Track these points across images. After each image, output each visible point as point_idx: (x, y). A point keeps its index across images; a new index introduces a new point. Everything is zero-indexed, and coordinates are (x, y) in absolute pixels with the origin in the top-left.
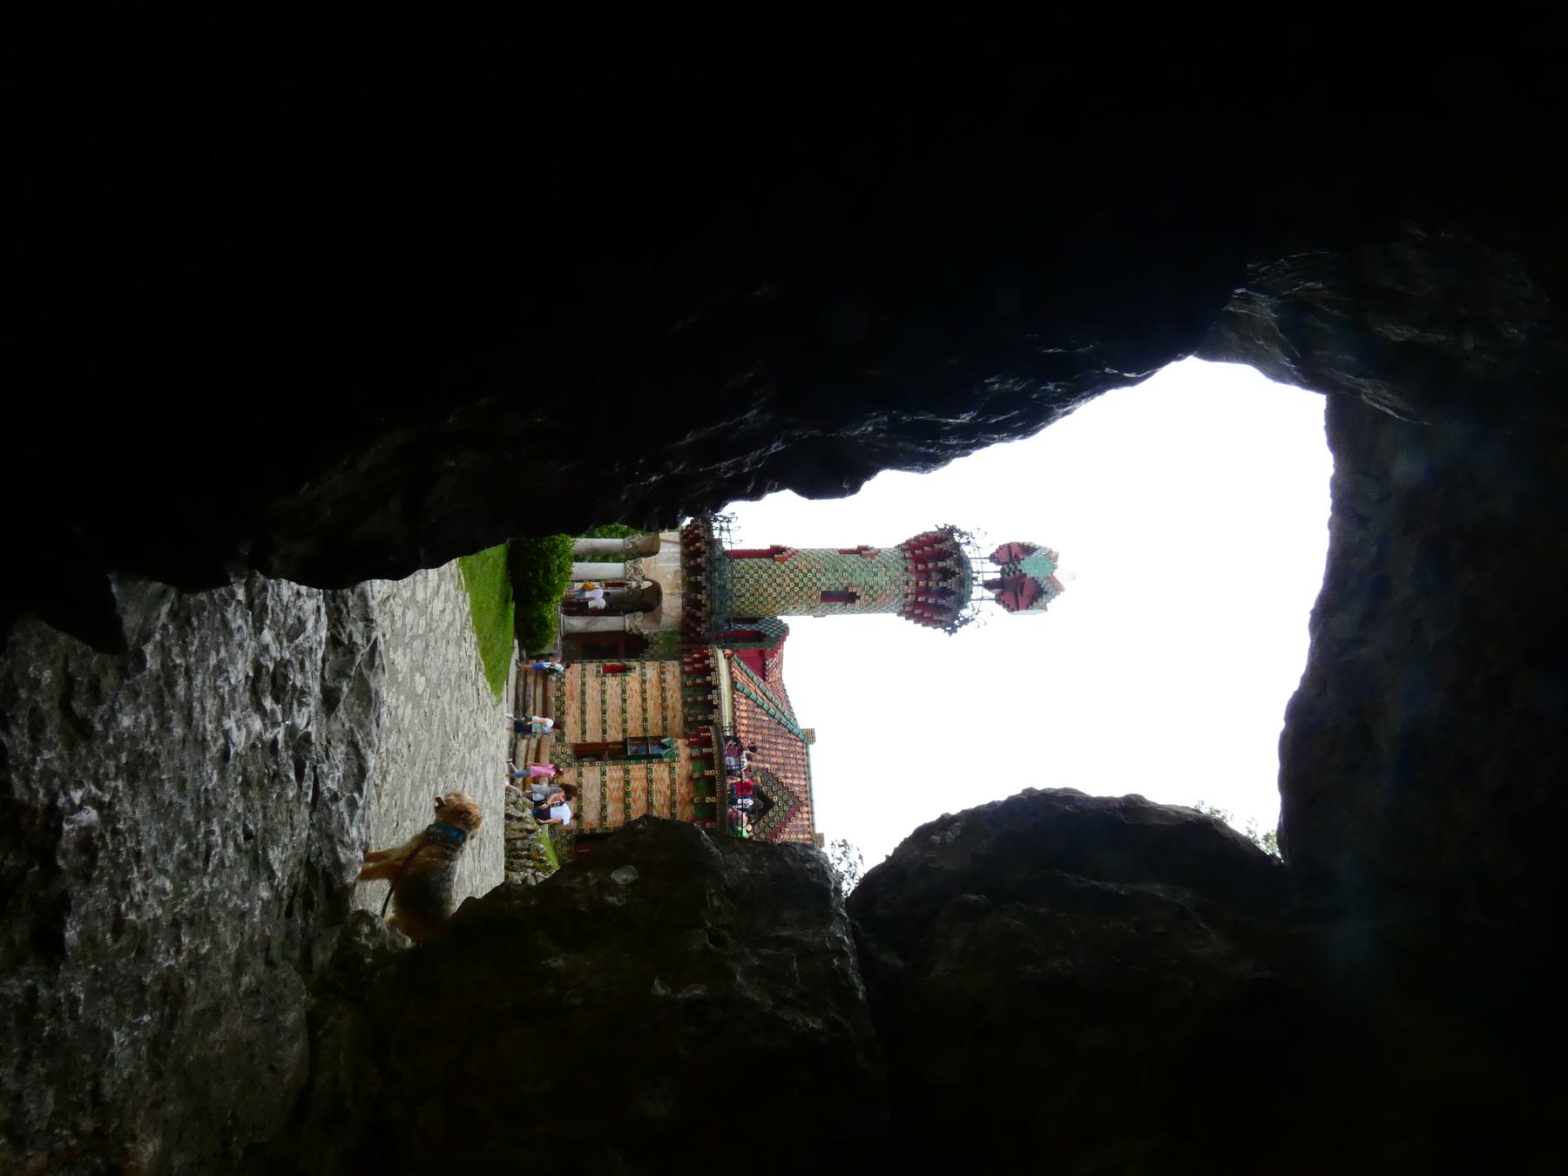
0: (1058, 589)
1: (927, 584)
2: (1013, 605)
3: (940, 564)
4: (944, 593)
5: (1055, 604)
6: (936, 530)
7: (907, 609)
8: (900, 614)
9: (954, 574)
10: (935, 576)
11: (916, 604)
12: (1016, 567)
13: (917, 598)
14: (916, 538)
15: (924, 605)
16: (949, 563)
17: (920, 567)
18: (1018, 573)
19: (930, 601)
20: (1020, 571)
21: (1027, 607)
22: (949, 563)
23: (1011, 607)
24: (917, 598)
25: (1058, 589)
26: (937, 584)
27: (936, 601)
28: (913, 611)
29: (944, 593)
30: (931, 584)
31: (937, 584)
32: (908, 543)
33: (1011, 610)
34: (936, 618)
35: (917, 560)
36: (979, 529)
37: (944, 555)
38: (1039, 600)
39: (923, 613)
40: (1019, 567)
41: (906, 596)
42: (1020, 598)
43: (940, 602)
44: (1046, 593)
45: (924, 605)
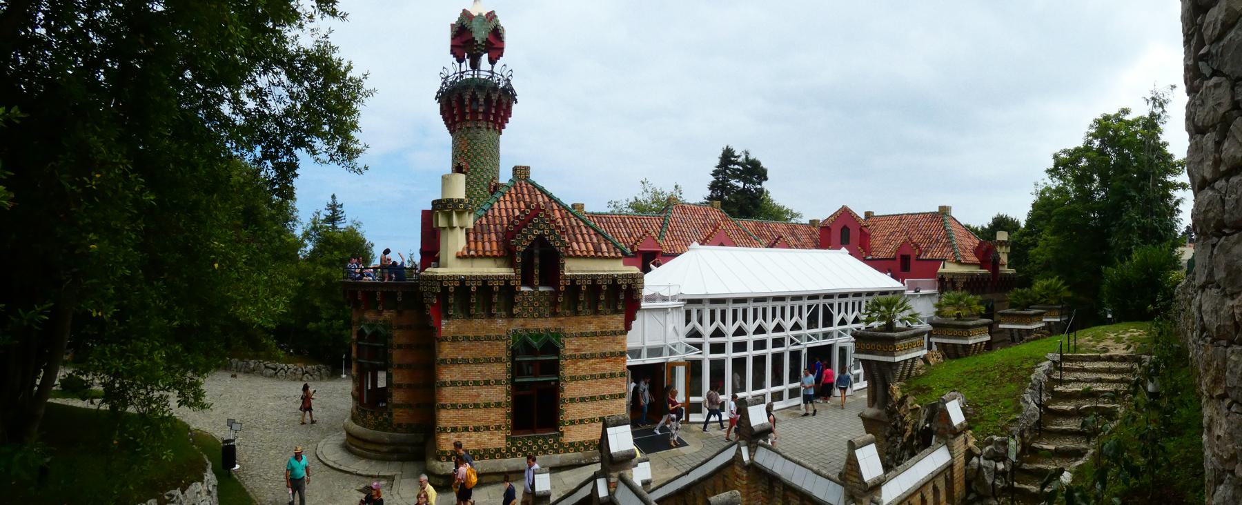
0: (491, 16)
1: (481, 112)
2: (500, 53)
3: (467, 102)
4: (488, 100)
6: (439, 104)
7: (497, 128)
8: (500, 133)
9: (474, 93)
10: (474, 106)
11: (495, 121)
13: (491, 121)
14: (445, 119)
15: (496, 116)
16: (467, 98)
17: (468, 118)
19: (493, 112)
22: (467, 98)
24: (491, 121)
25: (491, 16)
26: (481, 105)
29: (488, 100)
30: (481, 110)
31: (481, 105)
32: (449, 126)
33: (501, 55)
34: (504, 107)
35: (463, 119)
36: (441, 73)
37: (461, 100)
42: (495, 46)
43: (494, 104)
45: (496, 116)
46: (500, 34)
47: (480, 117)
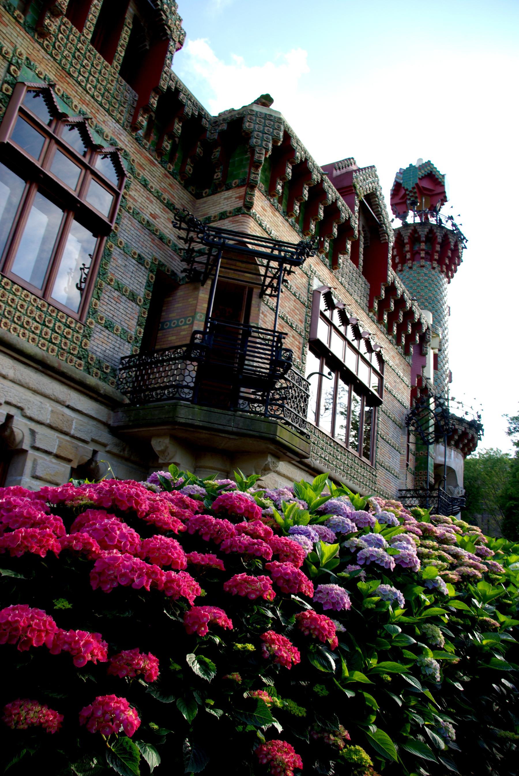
0: (429, 163)
5: (441, 167)
11: (440, 262)
12: (411, 192)
13: (436, 260)
17: (408, 256)
18: (415, 190)
20: (413, 188)
21: (443, 186)
23: (443, 198)
24: (436, 260)
27: (439, 243)
28: (446, 264)
38: (436, 177)
39: (448, 257)
40: (410, 189)
41: (434, 268)
42: (435, 192)
44: (431, 172)
46: (437, 179)
47: (423, 254)
